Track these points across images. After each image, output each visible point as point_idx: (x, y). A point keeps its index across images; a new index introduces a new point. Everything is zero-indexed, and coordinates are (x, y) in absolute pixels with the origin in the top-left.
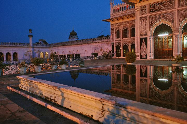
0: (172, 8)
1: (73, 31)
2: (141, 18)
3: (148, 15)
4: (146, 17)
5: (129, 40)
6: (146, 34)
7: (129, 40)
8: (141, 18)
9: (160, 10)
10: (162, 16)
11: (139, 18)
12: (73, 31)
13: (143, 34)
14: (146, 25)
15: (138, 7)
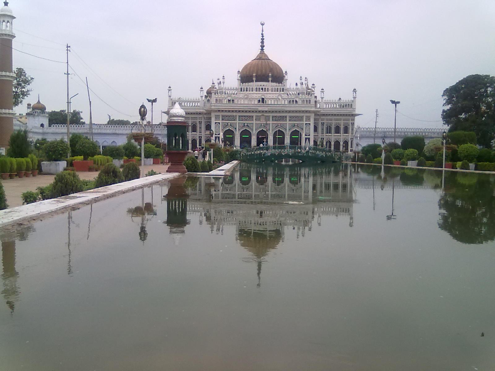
0: (234, 120)
1: (39, 102)
2: (216, 123)
3: (220, 122)
4: (219, 123)
5: (190, 135)
6: (219, 134)
7: (190, 135)
8: (216, 123)
9: (228, 120)
10: (229, 124)
11: (214, 123)
12: (39, 102)
13: (217, 134)
14: (219, 128)
15: (213, 115)
